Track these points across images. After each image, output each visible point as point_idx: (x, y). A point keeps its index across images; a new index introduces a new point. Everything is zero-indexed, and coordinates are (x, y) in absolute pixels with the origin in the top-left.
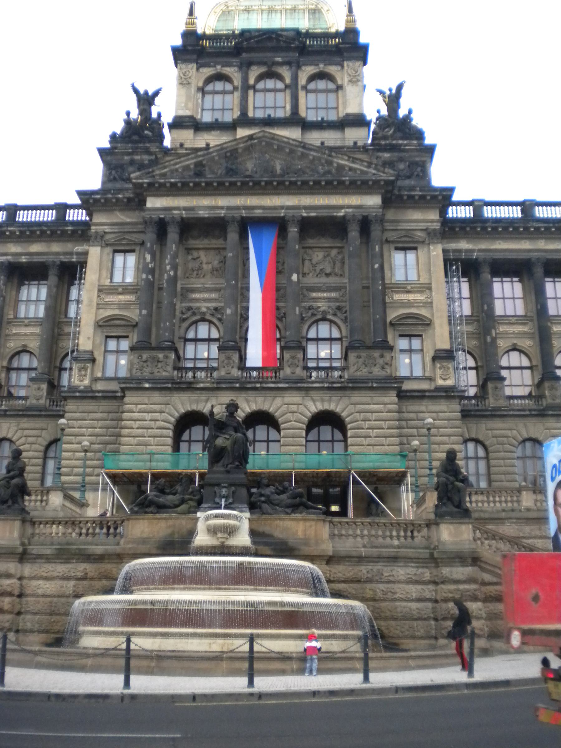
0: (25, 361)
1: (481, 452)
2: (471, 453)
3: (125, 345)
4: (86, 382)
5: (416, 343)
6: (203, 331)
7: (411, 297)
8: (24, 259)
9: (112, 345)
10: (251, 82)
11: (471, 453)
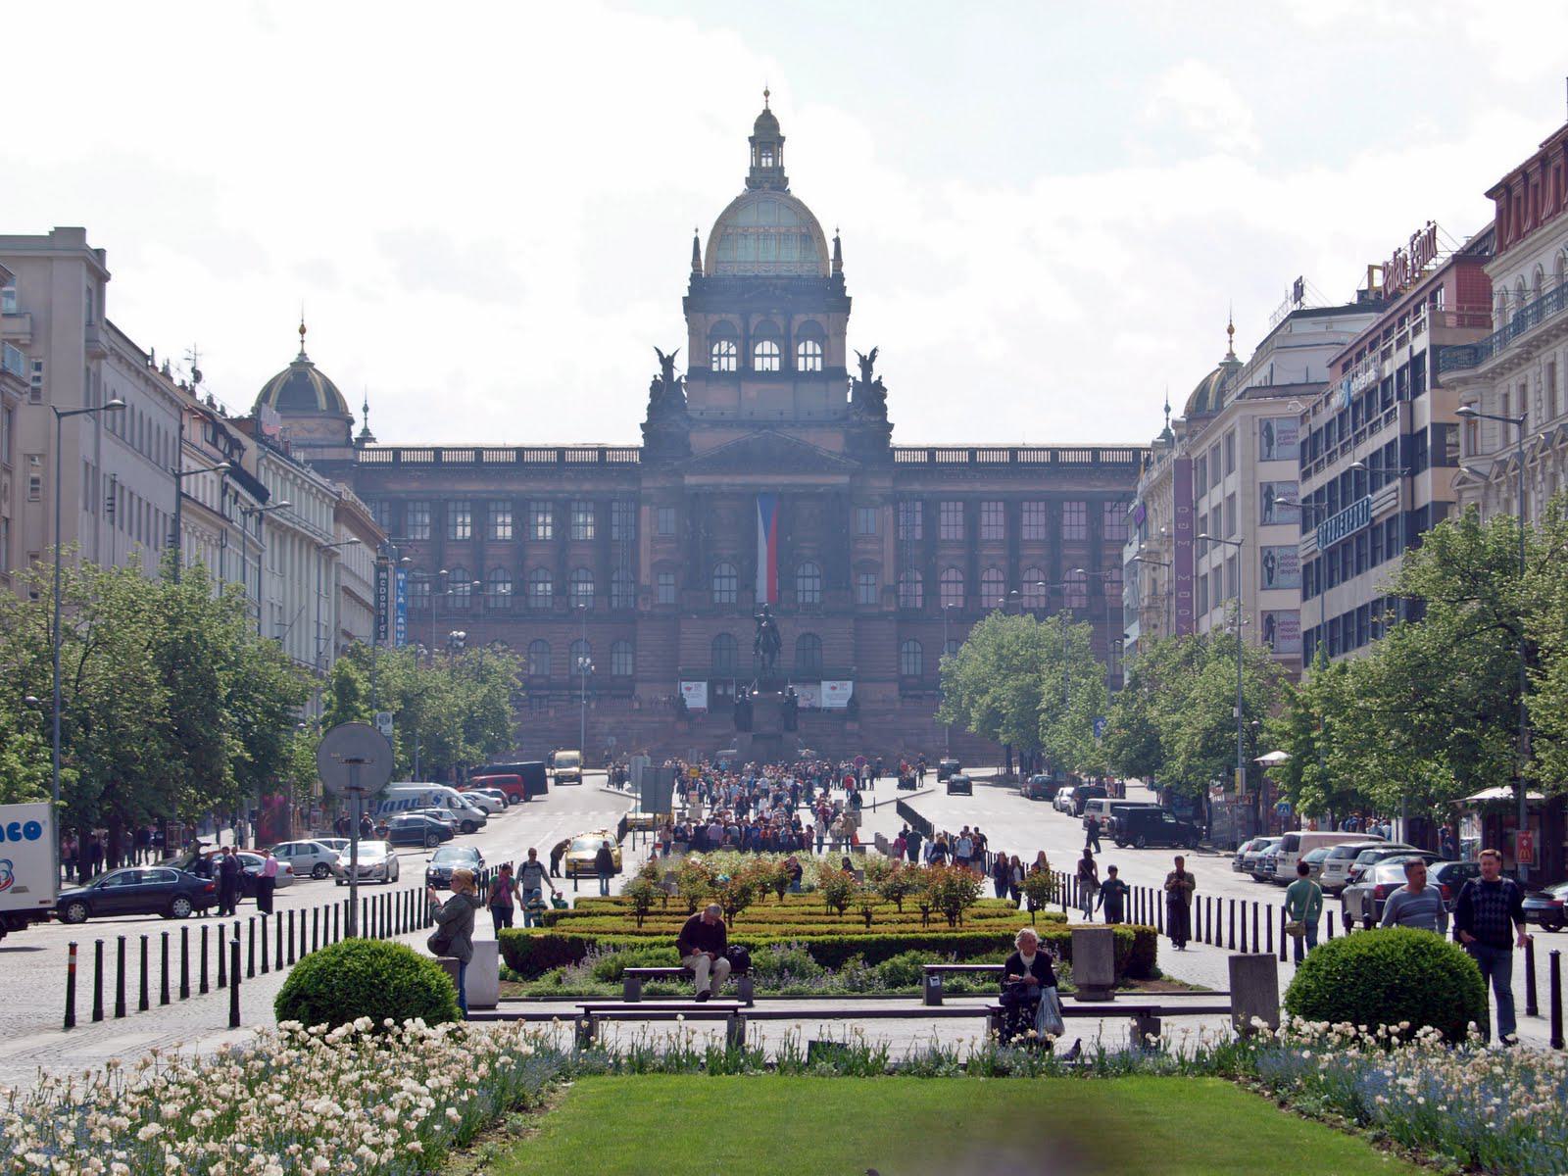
0: (582, 574)
1: (919, 649)
2: (912, 649)
3: (671, 579)
4: (648, 608)
5: (872, 580)
6: (725, 569)
7: (869, 547)
8: (578, 496)
9: (662, 580)
10: (752, 332)
11: (912, 649)
